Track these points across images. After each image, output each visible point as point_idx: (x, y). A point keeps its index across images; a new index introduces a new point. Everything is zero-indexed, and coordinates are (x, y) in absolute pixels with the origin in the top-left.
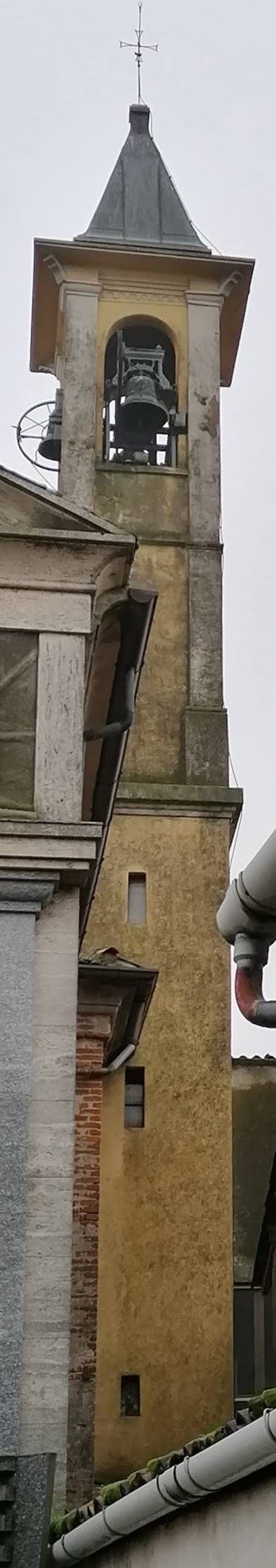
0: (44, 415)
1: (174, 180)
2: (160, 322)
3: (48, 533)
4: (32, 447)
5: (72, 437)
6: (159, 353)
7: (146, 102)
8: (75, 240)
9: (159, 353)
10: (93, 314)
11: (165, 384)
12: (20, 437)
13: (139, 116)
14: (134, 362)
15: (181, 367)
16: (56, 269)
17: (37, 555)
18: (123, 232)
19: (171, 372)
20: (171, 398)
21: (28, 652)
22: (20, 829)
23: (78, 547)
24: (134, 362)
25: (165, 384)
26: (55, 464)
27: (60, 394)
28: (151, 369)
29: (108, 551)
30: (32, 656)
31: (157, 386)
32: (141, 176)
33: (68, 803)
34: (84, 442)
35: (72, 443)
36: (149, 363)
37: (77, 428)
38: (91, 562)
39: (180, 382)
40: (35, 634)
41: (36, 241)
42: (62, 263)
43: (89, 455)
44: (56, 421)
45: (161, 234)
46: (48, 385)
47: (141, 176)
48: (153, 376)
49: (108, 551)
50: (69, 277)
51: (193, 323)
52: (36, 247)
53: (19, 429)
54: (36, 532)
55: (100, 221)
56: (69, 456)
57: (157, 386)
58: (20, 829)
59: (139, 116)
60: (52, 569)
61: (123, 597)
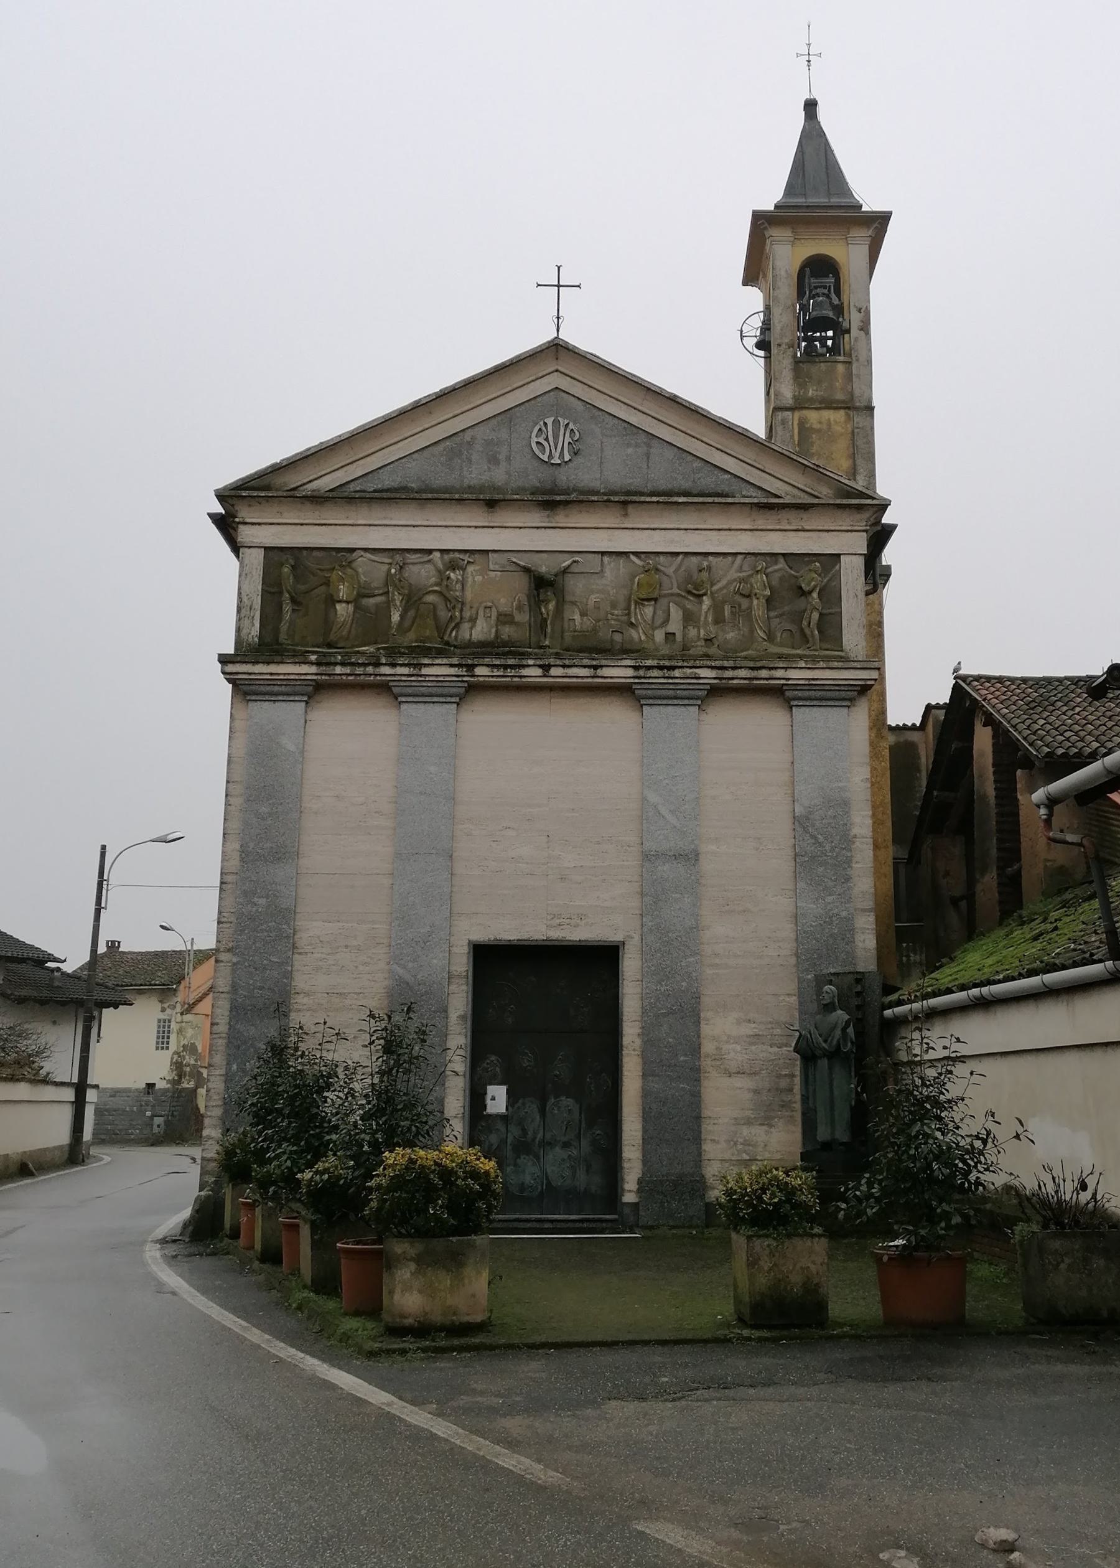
0: (757, 322)
1: (835, 152)
2: (831, 258)
3: (845, 501)
4: (751, 342)
5: (779, 341)
6: (831, 280)
7: (816, 95)
8: (776, 207)
9: (831, 280)
10: (788, 255)
11: (836, 301)
12: (742, 337)
13: (811, 106)
14: (816, 287)
15: (844, 288)
16: (766, 228)
17: (839, 513)
18: (805, 195)
19: (838, 293)
20: (839, 310)
21: (834, 567)
22: (840, 664)
23: (859, 508)
24: (816, 287)
25: (836, 301)
26: (762, 353)
27: (768, 309)
28: (826, 291)
29: (875, 509)
30: (837, 567)
31: (831, 303)
32: (814, 159)
33: (860, 647)
34: (787, 344)
35: (779, 345)
36: (825, 287)
37: (782, 336)
38: (866, 515)
39: (845, 297)
40: (839, 555)
41: (754, 212)
42: (770, 224)
43: (790, 352)
44: (766, 327)
45: (829, 195)
46: (755, 298)
47: (814, 159)
48: (828, 296)
49: (875, 509)
50: (775, 232)
51: (847, 253)
52: (753, 216)
53: (741, 331)
54: (838, 501)
55: (790, 189)
56: (778, 354)
57: (831, 303)
58: (840, 664)
59: (811, 106)
60: (845, 520)
61: (879, 528)
